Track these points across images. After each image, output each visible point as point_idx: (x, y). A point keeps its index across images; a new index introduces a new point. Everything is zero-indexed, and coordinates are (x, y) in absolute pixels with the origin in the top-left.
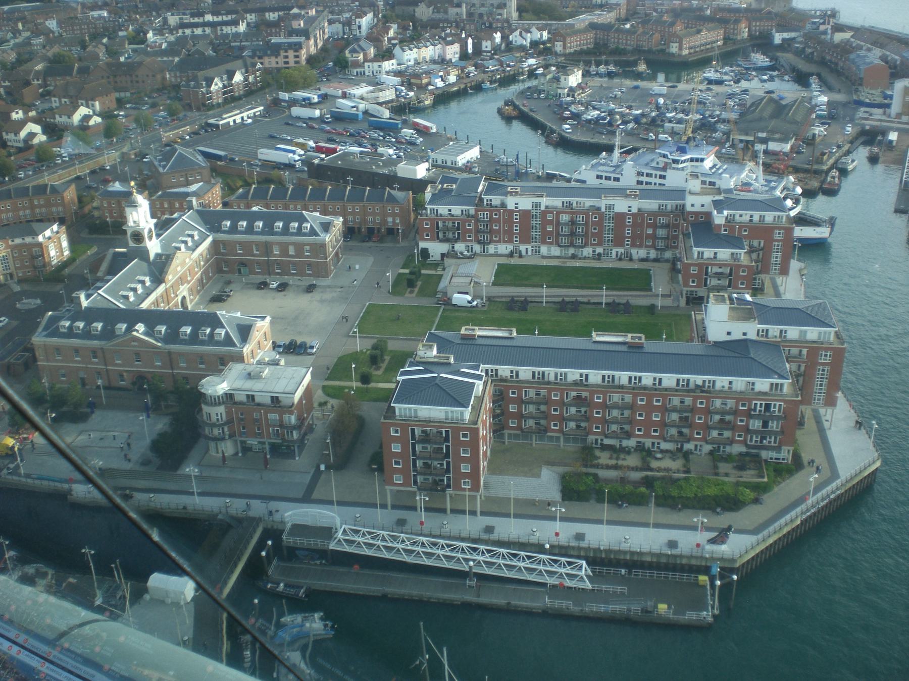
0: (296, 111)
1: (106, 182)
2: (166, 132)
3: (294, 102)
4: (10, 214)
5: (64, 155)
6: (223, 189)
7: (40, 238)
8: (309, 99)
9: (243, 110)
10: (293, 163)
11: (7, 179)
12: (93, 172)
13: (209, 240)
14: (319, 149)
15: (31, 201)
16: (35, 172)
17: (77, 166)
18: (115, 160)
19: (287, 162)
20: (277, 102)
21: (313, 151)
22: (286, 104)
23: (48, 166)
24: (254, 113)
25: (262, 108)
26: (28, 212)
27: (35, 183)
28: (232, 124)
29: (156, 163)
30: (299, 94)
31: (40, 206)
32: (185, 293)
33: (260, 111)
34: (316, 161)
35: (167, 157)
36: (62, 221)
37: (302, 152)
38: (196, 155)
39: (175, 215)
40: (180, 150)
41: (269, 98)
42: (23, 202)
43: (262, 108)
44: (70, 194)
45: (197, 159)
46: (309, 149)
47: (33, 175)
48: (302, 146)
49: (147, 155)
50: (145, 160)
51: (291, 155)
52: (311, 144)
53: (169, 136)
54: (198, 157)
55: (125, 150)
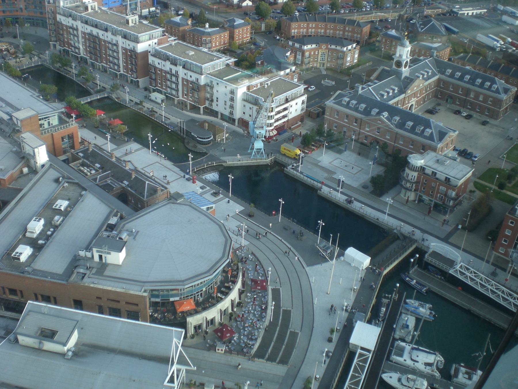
0: (505, 18)
1: (387, 28)
2: (427, 9)
3: (505, 12)
4: (332, 31)
5: (368, 7)
6: (451, 51)
7: (345, 49)
8: (515, 13)
9: (474, 8)
10: (495, 47)
11: (334, 11)
12: (381, 21)
13: (436, 78)
14: (512, 44)
15: (345, 27)
16: (350, 11)
17: (373, 15)
18: (395, 17)
19: (492, 46)
20: (495, 9)
21: (509, 44)
22: (500, 12)
23: (358, 11)
24: (481, 13)
25: (486, 10)
26: (341, 33)
27: (349, 18)
28: (466, 15)
29: (418, 25)
30: (510, 9)
31: (348, 31)
32: (414, 103)
33: (484, 12)
34: (510, 51)
35: (425, 24)
36: (358, 43)
37: (503, 43)
38: (442, 27)
39: (422, 58)
40: (434, 21)
41: (492, 6)
42: (340, 27)
43: (486, 10)
44: (366, 29)
45: (442, 29)
46: (507, 42)
47: (348, 13)
48: (504, 39)
49: (414, 19)
50: (411, 22)
51: (496, 43)
52: (510, 40)
53: (429, 12)
54: (443, 28)
55: (402, 13)
